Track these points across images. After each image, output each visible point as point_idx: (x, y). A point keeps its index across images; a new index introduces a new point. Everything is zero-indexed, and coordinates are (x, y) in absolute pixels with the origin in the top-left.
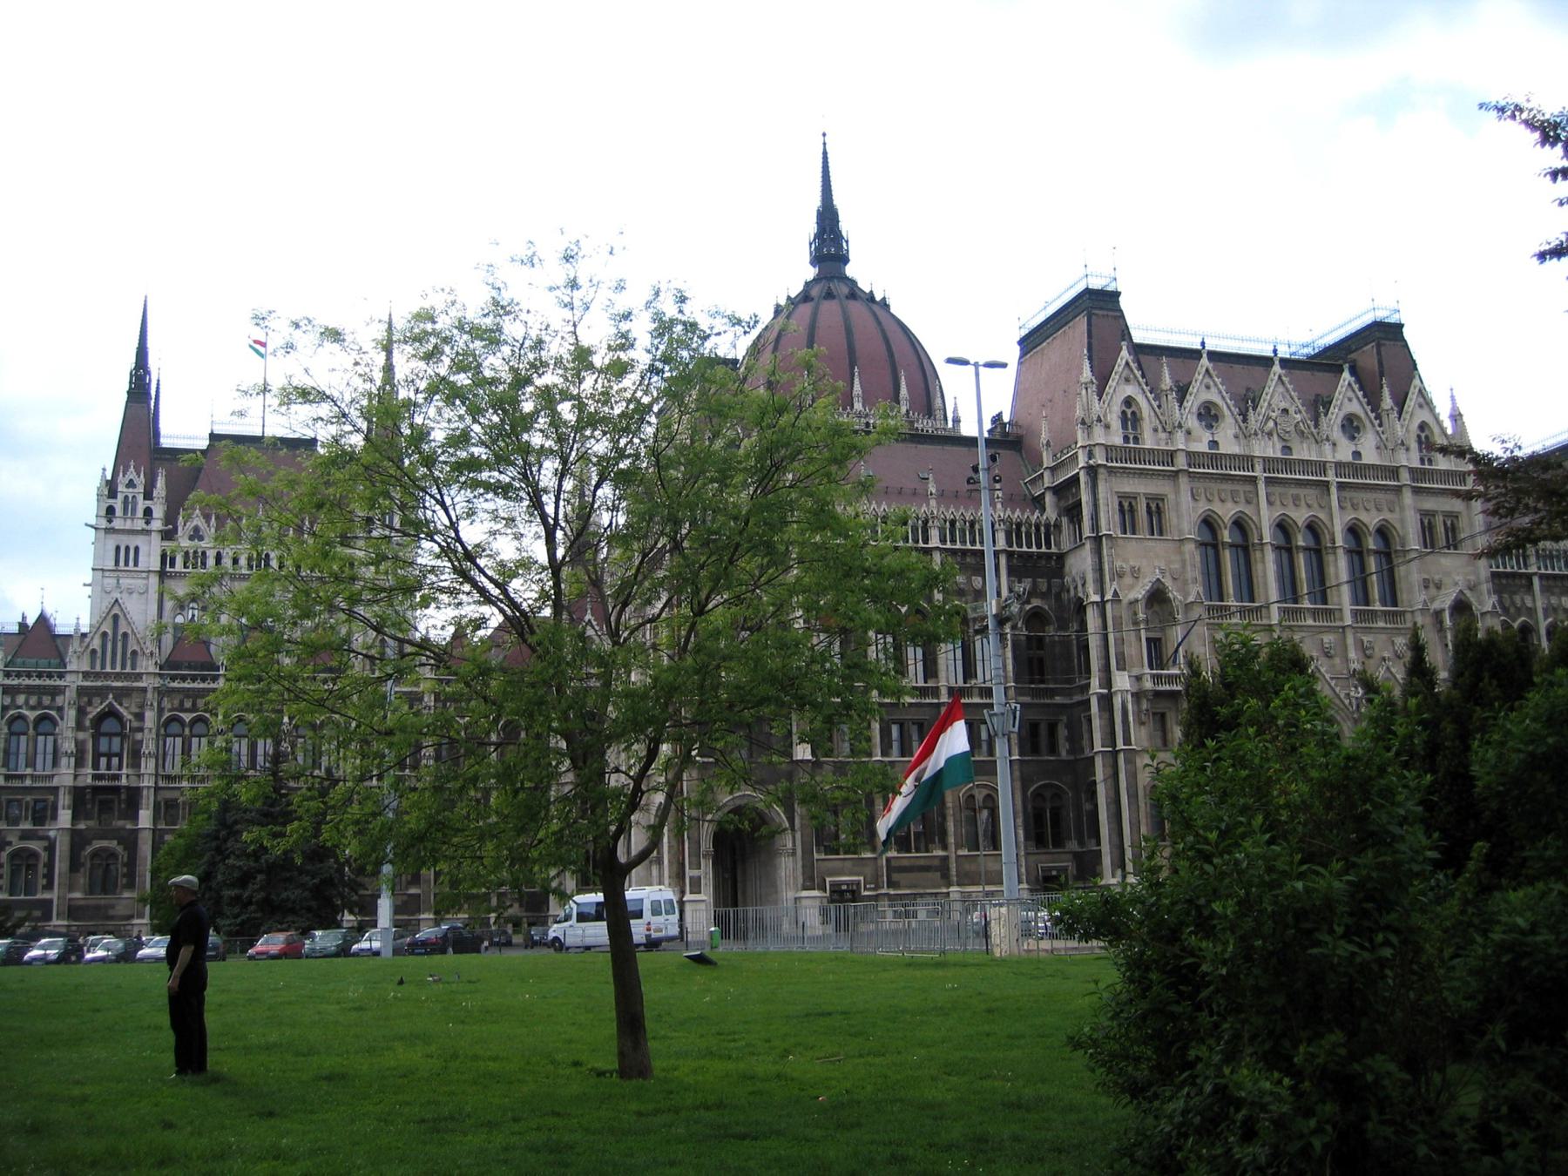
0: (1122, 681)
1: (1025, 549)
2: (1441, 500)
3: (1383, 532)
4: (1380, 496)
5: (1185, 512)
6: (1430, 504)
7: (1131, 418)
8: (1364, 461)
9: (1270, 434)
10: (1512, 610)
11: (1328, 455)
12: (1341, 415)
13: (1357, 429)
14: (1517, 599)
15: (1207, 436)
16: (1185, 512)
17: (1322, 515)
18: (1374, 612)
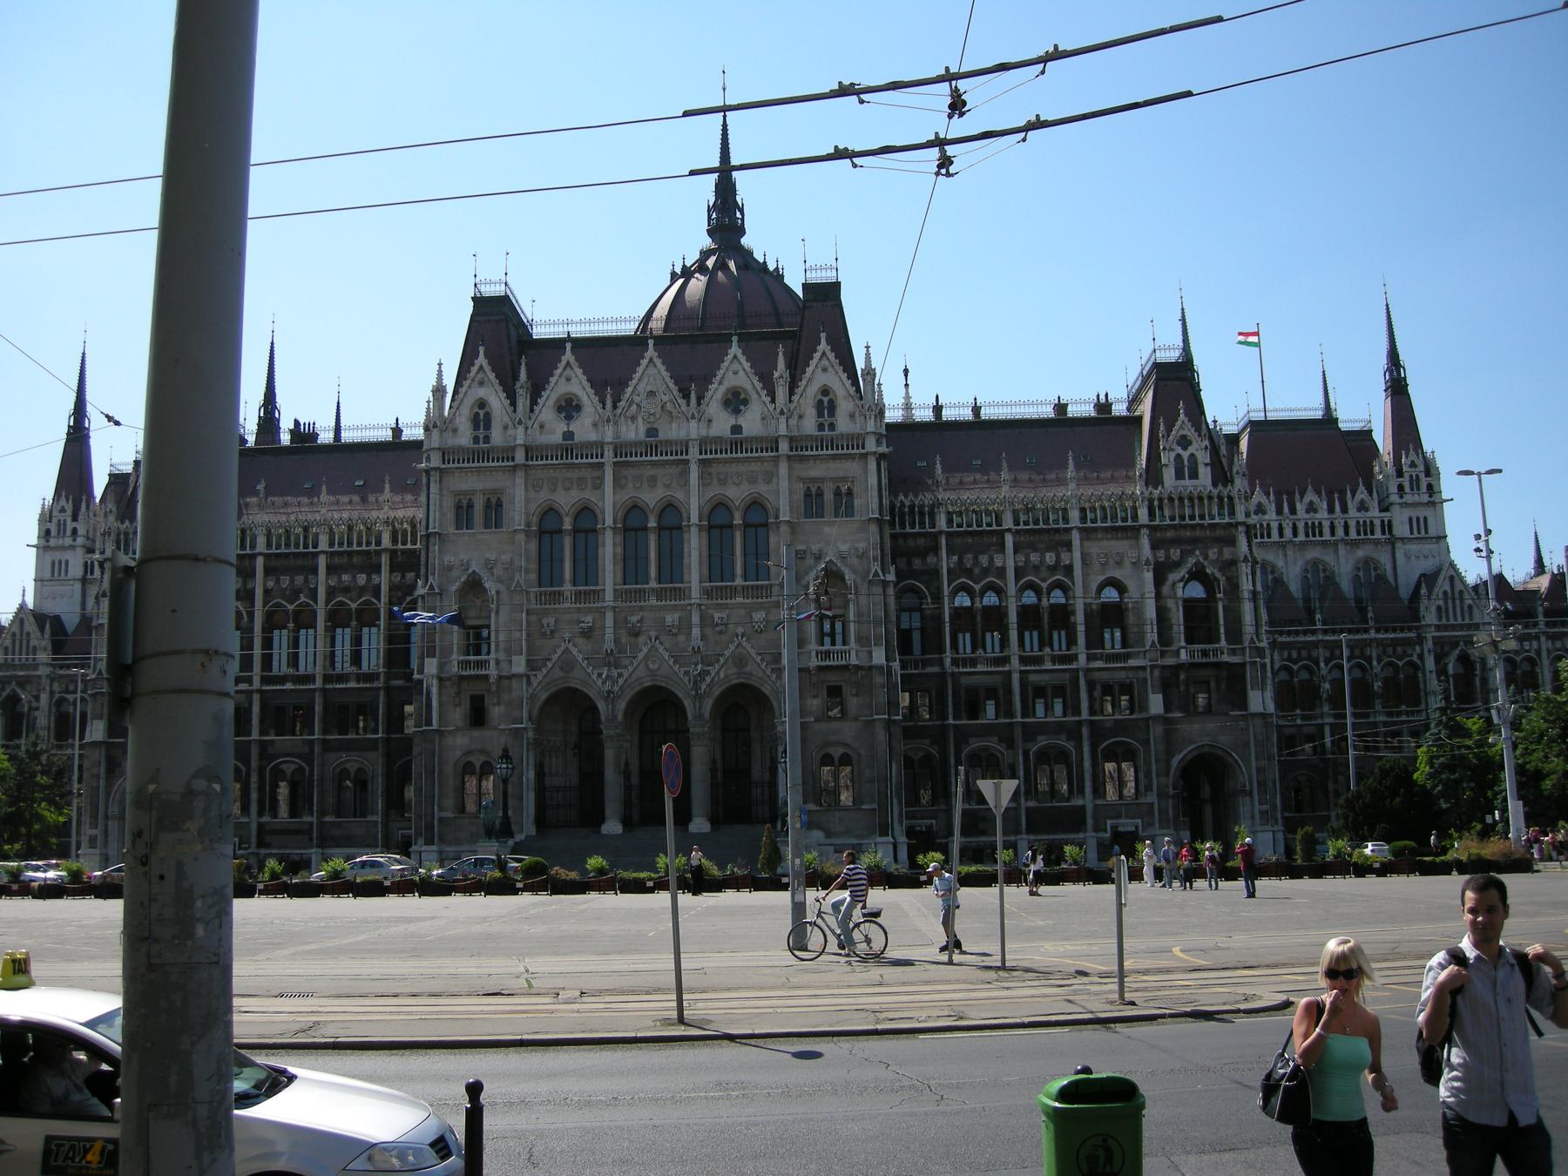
0: (431, 666)
1: (409, 546)
2: (832, 465)
3: (756, 504)
4: (755, 467)
5: (521, 503)
6: (817, 470)
7: (482, 420)
8: (746, 433)
9: (633, 418)
10: (977, 571)
11: (694, 430)
12: (722, 389)
13: (745, 402)
14: (984, 560)
15: (562, 427)
16: (521, 503)
17: (680, 495)
18: (733, 591)
